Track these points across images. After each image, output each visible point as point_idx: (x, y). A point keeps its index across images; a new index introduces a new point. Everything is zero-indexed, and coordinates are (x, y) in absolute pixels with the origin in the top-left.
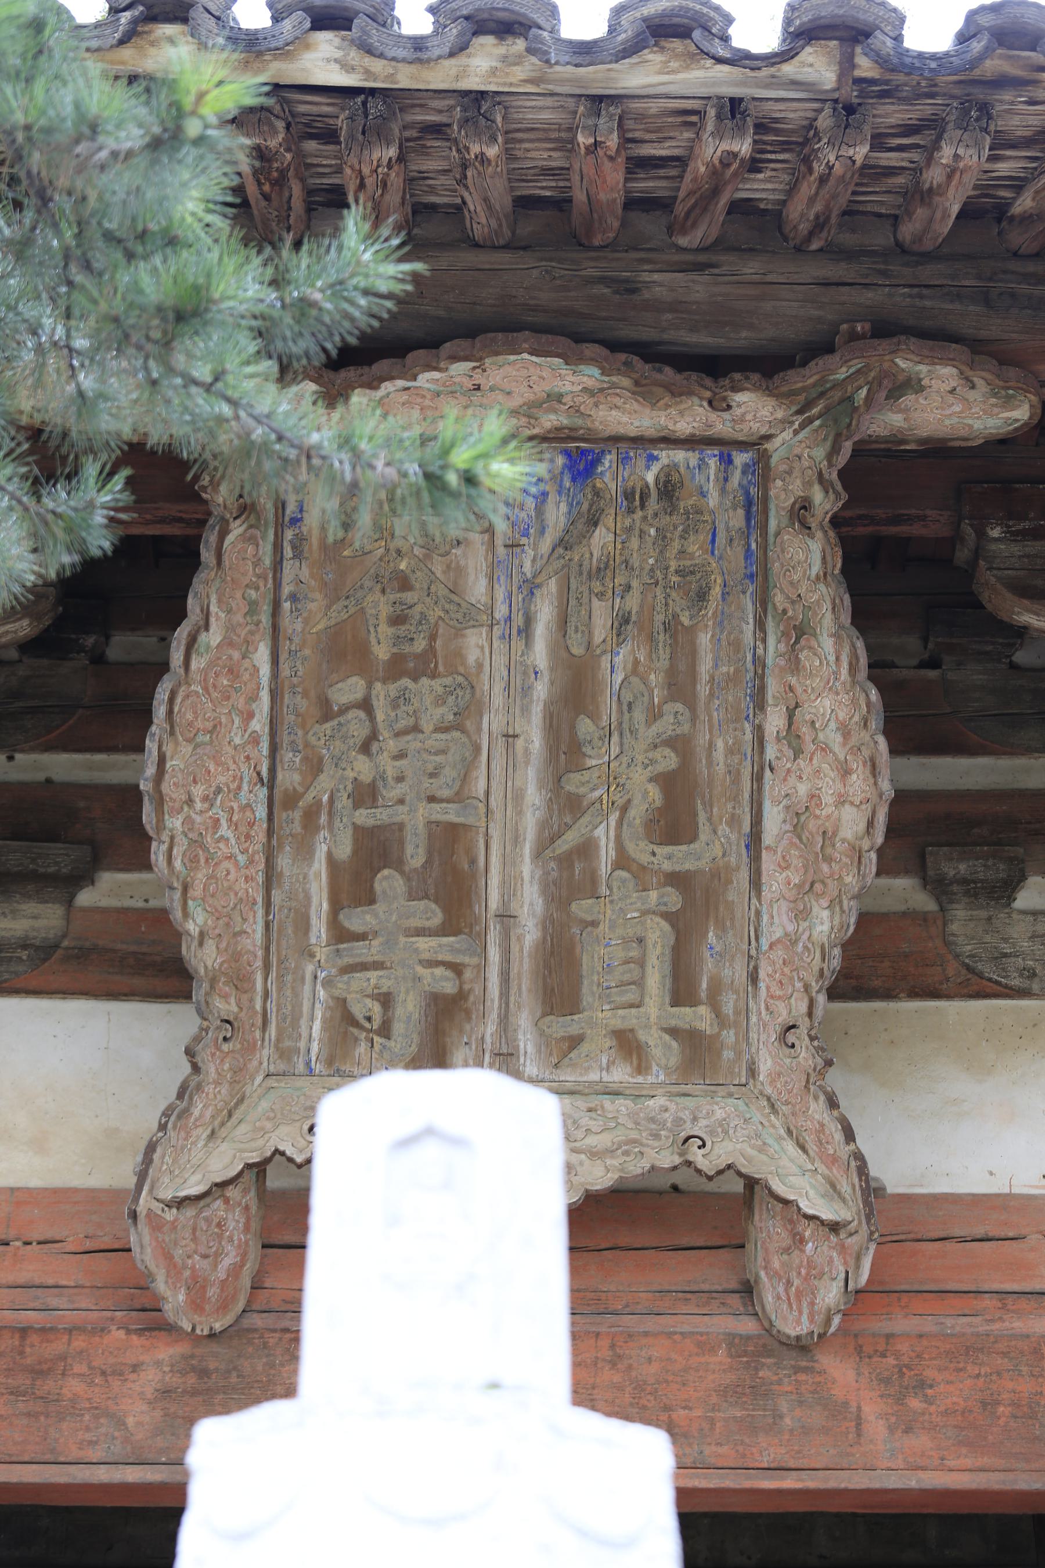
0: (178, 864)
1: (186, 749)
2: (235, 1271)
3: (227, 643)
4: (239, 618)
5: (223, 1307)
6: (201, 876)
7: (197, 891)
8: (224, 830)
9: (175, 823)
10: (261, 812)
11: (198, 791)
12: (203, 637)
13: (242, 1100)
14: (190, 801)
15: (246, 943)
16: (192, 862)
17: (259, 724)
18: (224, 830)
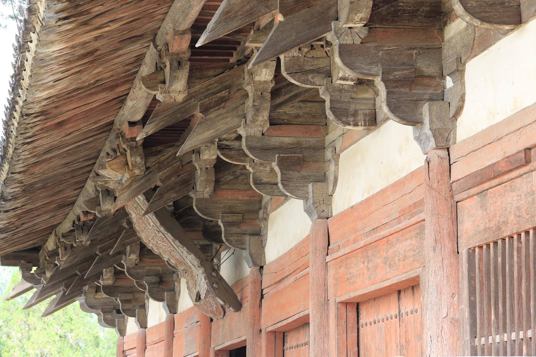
0: (156, 251)
1: (143, 234)
2: (217, 308)
3: (136, 215)
4: (135, 211)
5: (220, 314)
6: (161, 251)
7: (162, 254)
8: (159, 242)
9: (151, 245)
10: (163, 236)
11: (150, 239)
12: (132, 216)
13: (196, 281)
14: (150, 241)
15: (177, 257)
16: (158, 249)
17: (152, 224)
18: (159, 242)
